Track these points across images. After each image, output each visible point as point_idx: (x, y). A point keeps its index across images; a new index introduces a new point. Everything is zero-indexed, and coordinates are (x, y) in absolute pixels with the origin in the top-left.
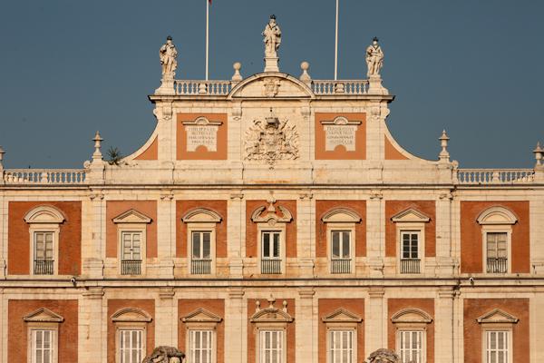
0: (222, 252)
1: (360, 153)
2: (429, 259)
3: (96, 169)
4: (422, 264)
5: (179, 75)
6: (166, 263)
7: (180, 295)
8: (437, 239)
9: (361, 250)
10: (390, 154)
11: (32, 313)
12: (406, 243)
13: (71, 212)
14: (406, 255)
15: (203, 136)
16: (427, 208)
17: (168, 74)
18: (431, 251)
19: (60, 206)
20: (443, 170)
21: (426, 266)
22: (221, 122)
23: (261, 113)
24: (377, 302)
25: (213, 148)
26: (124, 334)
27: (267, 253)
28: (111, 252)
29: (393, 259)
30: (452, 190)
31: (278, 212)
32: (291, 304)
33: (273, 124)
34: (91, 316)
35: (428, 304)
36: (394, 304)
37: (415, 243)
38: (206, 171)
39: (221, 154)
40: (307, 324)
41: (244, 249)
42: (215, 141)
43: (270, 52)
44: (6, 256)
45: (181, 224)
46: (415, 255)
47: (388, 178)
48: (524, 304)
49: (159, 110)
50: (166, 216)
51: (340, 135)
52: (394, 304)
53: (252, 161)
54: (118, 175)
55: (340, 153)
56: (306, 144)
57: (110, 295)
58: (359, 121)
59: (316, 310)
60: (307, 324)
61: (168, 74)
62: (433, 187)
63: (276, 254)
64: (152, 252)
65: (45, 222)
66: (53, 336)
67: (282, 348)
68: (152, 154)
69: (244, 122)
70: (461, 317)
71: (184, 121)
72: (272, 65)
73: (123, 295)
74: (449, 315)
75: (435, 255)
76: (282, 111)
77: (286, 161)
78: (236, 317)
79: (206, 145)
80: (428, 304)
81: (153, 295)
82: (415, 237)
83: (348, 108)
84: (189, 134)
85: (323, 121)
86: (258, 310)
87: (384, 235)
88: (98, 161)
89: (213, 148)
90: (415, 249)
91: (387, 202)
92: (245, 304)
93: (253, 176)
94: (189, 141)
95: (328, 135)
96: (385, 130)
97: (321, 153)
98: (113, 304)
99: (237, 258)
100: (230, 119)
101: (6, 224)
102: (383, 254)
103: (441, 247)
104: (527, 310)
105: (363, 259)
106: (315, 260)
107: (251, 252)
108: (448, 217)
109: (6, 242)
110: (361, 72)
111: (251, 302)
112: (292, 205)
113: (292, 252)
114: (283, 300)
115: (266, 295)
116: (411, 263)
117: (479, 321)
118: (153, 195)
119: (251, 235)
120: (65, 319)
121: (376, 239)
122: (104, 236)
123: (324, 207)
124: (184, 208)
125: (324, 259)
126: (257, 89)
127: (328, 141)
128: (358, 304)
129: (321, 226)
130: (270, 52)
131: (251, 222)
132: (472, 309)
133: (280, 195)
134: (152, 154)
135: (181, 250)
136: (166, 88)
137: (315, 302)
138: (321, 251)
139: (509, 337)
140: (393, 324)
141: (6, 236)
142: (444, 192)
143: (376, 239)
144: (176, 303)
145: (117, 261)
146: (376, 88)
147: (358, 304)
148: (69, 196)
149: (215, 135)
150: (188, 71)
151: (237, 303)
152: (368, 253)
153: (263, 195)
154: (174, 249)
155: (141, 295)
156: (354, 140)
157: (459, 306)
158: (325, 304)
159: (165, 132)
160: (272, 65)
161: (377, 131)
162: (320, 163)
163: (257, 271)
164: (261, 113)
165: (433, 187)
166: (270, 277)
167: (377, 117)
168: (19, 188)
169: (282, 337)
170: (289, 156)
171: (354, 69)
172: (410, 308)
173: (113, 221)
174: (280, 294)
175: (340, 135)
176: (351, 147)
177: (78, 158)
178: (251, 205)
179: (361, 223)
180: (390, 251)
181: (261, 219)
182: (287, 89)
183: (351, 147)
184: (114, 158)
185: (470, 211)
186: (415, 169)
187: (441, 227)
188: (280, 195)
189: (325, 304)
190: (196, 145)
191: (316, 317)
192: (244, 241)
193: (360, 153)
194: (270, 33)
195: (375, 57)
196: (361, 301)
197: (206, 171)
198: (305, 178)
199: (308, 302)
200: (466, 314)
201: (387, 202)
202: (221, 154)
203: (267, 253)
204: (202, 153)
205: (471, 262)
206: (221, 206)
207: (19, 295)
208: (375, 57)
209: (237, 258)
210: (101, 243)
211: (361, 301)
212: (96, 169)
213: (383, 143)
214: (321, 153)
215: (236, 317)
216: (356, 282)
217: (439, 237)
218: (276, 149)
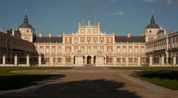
0: (85, 42)
1: (97, 33)
3: (73, 34)
5: (81, 25)
6: (79, 43)
9: (97, 42)
10: (100, 33)
13: (71, 38)
15: (83, 31)
16: (103, 38)
17: (80, 25)
18: (104, 42)
19: (70, 37)
20: (105, 34)
21: (103, 43)
22: (84, 30)
23: (88, 29)
25: (84, 32)
26: (76, 49)
28: (74, 42)
32: (91, 46)
33: (89, 30)
34: (73, 48)
35: (104, 46)
36: (100, 46)
38: (83, 34)
39: (84, 33)
40: (92, 48)
43: (89, 23)
45: (81, 39)
47: (100, 35)
48: (112, 46)
49: (79, 29)
50: (79, 38)
51: (95, 31)
52: (100, 46)
54: (75, 35)
55: (95, 33)
56: (92, 31)
57: (74, 46)
58: (97, 30)
60: (92, 48)
61: (80, 25)
62: (104, 36)
64: (78, 42)
65: (68, 39)
66: (69, 49)
67: (90, 51)
68: (78, 33)
69: (87, 30)
71: (81, 30)
72: (89, 25)
73: (76, 46)
74: (105, 47)
76: (90, 29)
77: (90, 33)
78: (86, 48)
83: (96, 28)
85: (94, 30)
88: (73, 33)
93: (87, 35)
96: (99, 30)
97: (94, 33)
99: (86, 42)
103: (105, 41)
107: (87, 42)
108: (105, 38)
110: (97, 25)
111: (87, 46)
112: (91, 37)
113: (91, 42)
115: (89, 46)
119: (87, 40)
120: (70, 48)
121: (99, 40)
123: (94, 38)
124: (81, 38)
126: (88, 27)
128: (97, 46)
129: (94, 39)
130: (89, 23)
131: (87, 39)
132: (108, 47)
133: (90, 37)
134: (78, 33)
135: (81, 42)
136: (79, 27)
138: (94, 42)
140: (100, 48)
143: (99, 40)
145: (75, 43)
146: (99, 27)
147: (97, 46)
148: (71, 37)
150: (81, 25)
153: (88, 36)
155: (77, 46)
157: (106, 46)
158: (94, 46)
159: (79, 31)
160: (89, 25)
161: (99, 31)
162: (94, 34)
163: (88, 43)
164: (88, 29)
165: (104, 36)
166: (89, 44)
167: (99, 29)
168: (66, 36)
169: (90, 49)
171: (97, 25)
173: (74, 39)
175: (95, 31)
176: (96, 32)
177: (71, 33)
178: (87, 37)
179: (97, 39)
180: (100, 42)
182: (91, 27)
183: (96, 32)
184: (75, 33)
185: (107, 38)
186: (102, 34)
187: (105, 39)
188: (90, 37)
189: (94, 46)
193: (97, 33)
194: (89, 21)
195: (99, 24)
197: (83, 34)
198: (92, 35)
202: (84, 33)
204: (83, 33)
205: (107, 43)
206: (85, 37)
207: (66, 46)
208: (99, 24)
209: (86, 42)
210: (74, 41)
212: (73, 34)
214: (94, 33)
215: (86, 48)
216: (97, 44)
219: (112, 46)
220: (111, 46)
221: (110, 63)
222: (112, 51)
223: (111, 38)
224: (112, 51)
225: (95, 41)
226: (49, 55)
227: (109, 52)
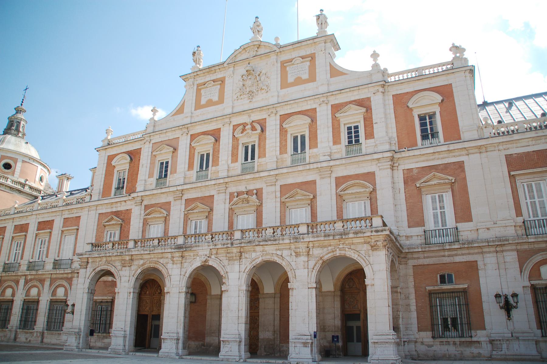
2: (368, 141)
4: (363, 146)
7: (186, 197)
8: (374, 125)
11: (106, 220)
12: (350, 133)
14: (350, 142)
18: (370, 135)
24: (327, 180)
27: (246, 159)
29: (338, 146)
30: (383, 86)
31: (253, 129)
32: (259, 193)
36: (340, 181)
37: (357, 132)
41: (230, 157)
42: (217, 94)
44: (102, 187)
46: (357, 141)
48: (460, 166)
52: (340, 181)
53: (239, 101)
56: (275, 80)
57: (145, 203)
59: (278, 194)
63: (253, 158)
70: (401, 185)
75: (374, 138)
79: (212, 98)
80: (370, 177)
81: (170, 199)
82: (356, 127)
84: (203, 94)
86: (235, 199)
87: (331, 129)
89: (216, 98)
90: (357, 136)
91: (332, 105)
92: (228, 197)
94: (203, 98)
95: (289, 72)
97: (284, 84)
98: (147, 207)
100: (227, 79)
101: (105, 169)
102: (331, 143)
103: (379, 130)
104: (463, 171)
105: (315, 150)
106: (279, 157)
109: (103, 179)
114: (253, 190)
115: (242, 188)
116: (354, 148)
117: (418, 185)
118: (177, 134)
119: (235, 148)
122: (149, 166)
125: (285, 156)
127: (289, 76)
129: (283, 132)
137: (278, 188)
139: (448, 198)
141: (104, 176)
142: (377, 88)
144: (184, 202)
149: (217, 91)
151: (222, 196)
152: (319, 145)
154: (187, 166)
156: (307, 71)
170: (263, 91)
172: (353, 182)
174: (251, 187)
176: (305, 76)
180: (336, 141)
181: (241, 135)
183: (305, 76)
190: (206, 100)
191: (279, 200)
192: (230, 152)
196: (314, 182)
199: (272, 189)
200: (405, 183)
201: (332, 105)
202: (221, 100)
203: (246, 159)
211: (314, 182)
213: (328, 68)
217: (376, 123)
218: (254, 89)
219: (460, 166)
220: (444, 168)
221: (452, 350)
222: (464, 212)
223: (439, 98)
224: (464, 212)
225: (299, 144)
226: (17, 282)
227: (430, 225)
